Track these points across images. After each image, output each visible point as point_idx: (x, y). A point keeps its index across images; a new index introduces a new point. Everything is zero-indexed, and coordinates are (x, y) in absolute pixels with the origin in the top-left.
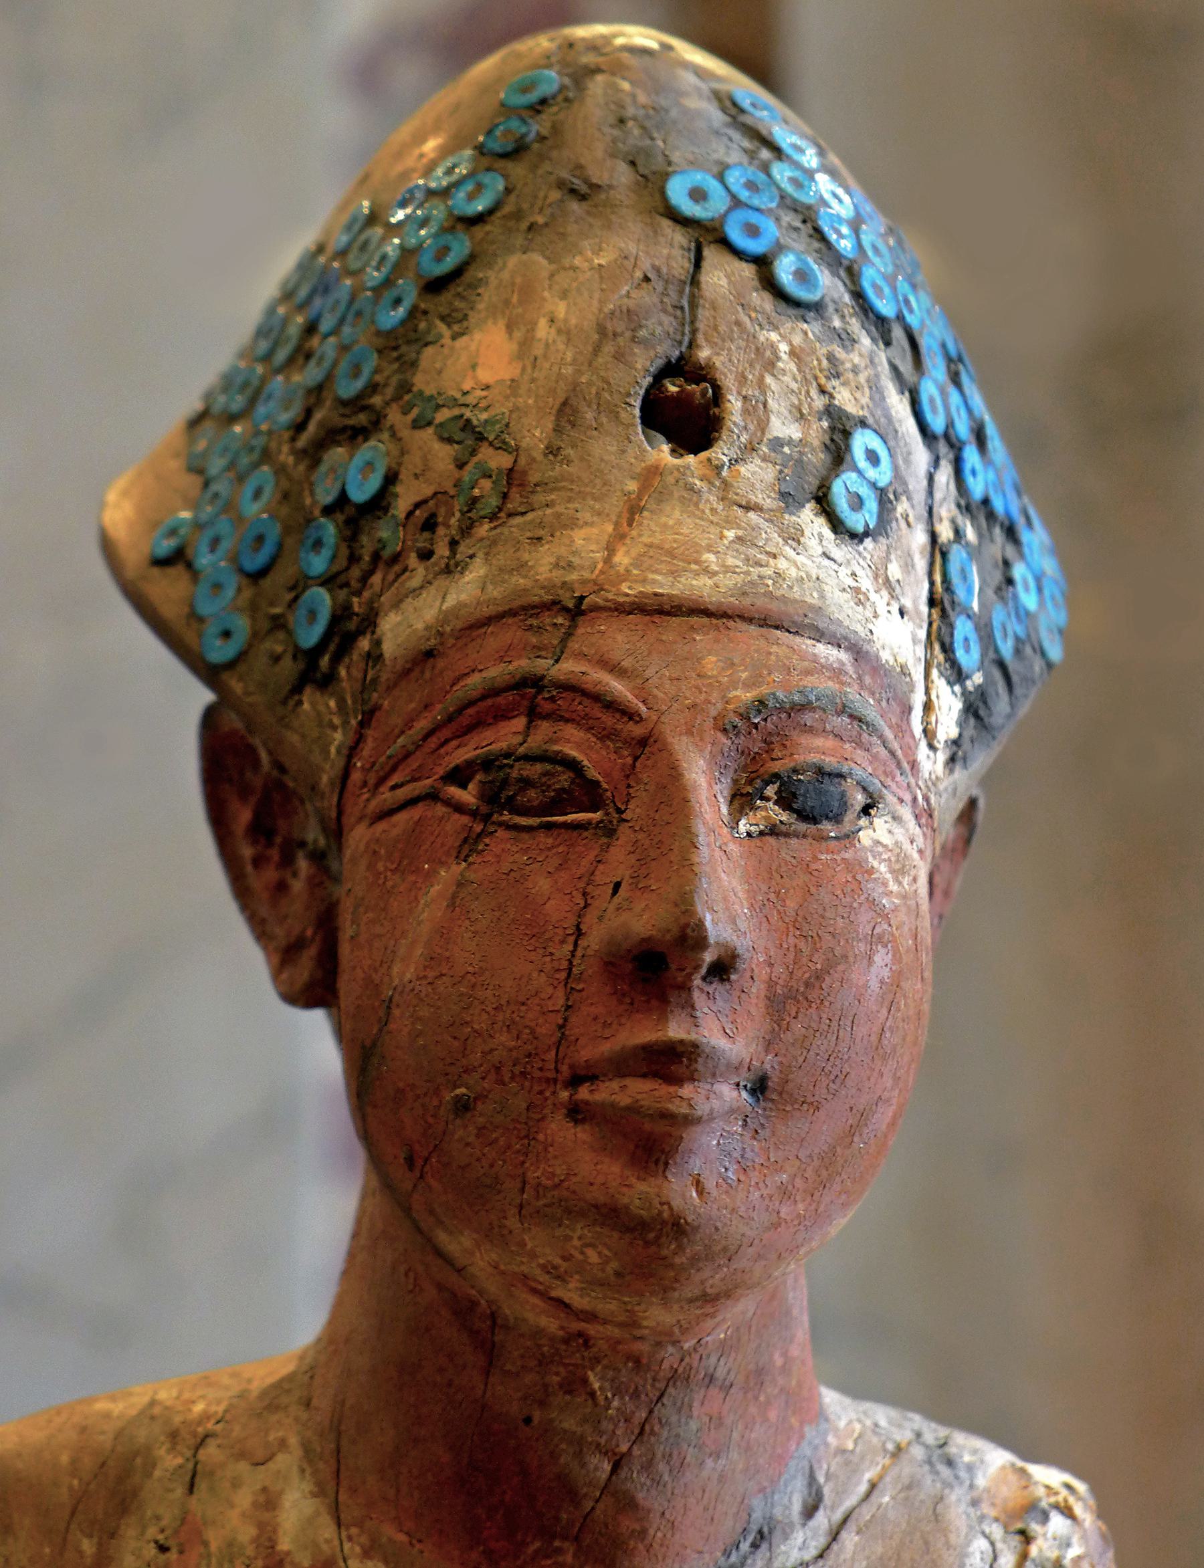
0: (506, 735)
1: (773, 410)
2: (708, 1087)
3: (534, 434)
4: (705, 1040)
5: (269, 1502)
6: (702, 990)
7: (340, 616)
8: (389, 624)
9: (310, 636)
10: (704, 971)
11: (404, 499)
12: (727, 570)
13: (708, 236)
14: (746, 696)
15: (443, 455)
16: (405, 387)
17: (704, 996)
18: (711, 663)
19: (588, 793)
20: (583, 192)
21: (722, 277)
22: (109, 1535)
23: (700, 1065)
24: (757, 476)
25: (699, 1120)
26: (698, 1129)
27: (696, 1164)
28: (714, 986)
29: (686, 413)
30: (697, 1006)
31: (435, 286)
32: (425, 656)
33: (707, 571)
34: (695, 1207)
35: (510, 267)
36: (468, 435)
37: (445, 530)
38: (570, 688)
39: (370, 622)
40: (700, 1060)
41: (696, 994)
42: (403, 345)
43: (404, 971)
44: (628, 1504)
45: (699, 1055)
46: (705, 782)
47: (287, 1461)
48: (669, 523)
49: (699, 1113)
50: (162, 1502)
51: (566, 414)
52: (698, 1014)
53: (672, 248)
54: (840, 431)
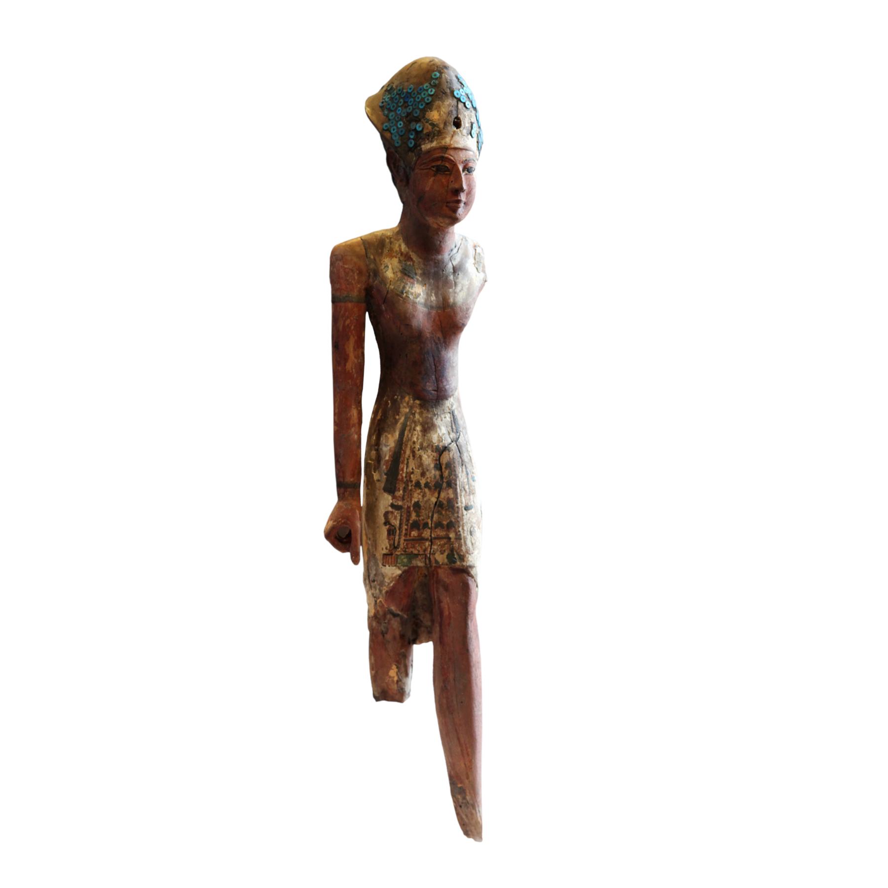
0: (439, 163)
1: (465, 123)
3: (442, 126)
5: (400, 246)
7: (415, 144)
8: (423, 146)
9: (411, 146)
11: (425, 132)
13: (459, 100)
15: (430, 127)
16: (424, 117)
19: (448, 170)
20: (445, 93)
21: (461, 105)
22: (382, 249)
24: (465, 132)
29: (458, 124)
31: (427, 104)
32: (428, 152)
35: (437, 103)
36: (433, 125)
37: (430, 136)
38: (447, 158)
39: (420, 145)
42: (424, 111)
43: (427, 189)
44: (441, 247)
47: (401, 241)
48: (456, 138)
50: (388, 246)
51: (445, 124)
53: (454, 102)
54: (472, 124)
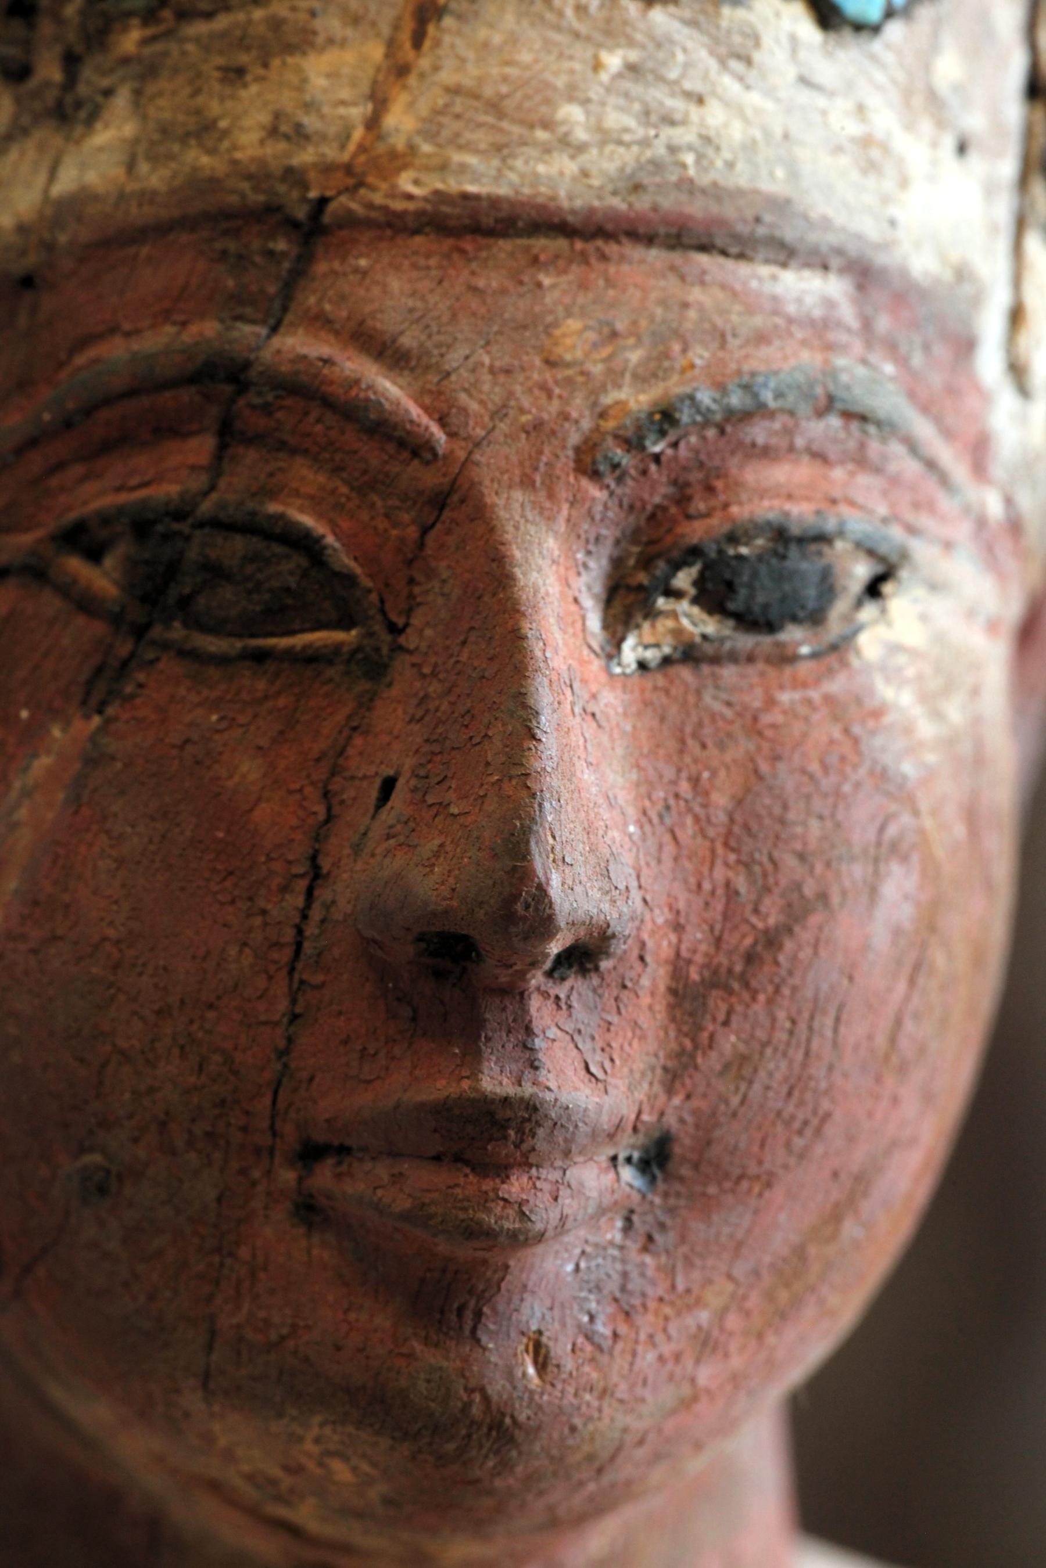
2: (556, 1175)
4: (549, 1097)
6: (546, 995)
10: (548, 965)
12: (606, 137)
14: (636, 399)
17: (550, 1004)
18: (575, 337)
23: (540, 1142)
25: (541, 1237)
26: (540, 1249)
27: (533, 1313)
28: (568, 984)
30: (537, 1026)
33: (565, 142)
34: (532, 1393)
40: (541, 1132)
41: (535, 1003)
45: (538, 1124)
46: (558, 582)
49: (539, 1226)
52: (538, 1043)
